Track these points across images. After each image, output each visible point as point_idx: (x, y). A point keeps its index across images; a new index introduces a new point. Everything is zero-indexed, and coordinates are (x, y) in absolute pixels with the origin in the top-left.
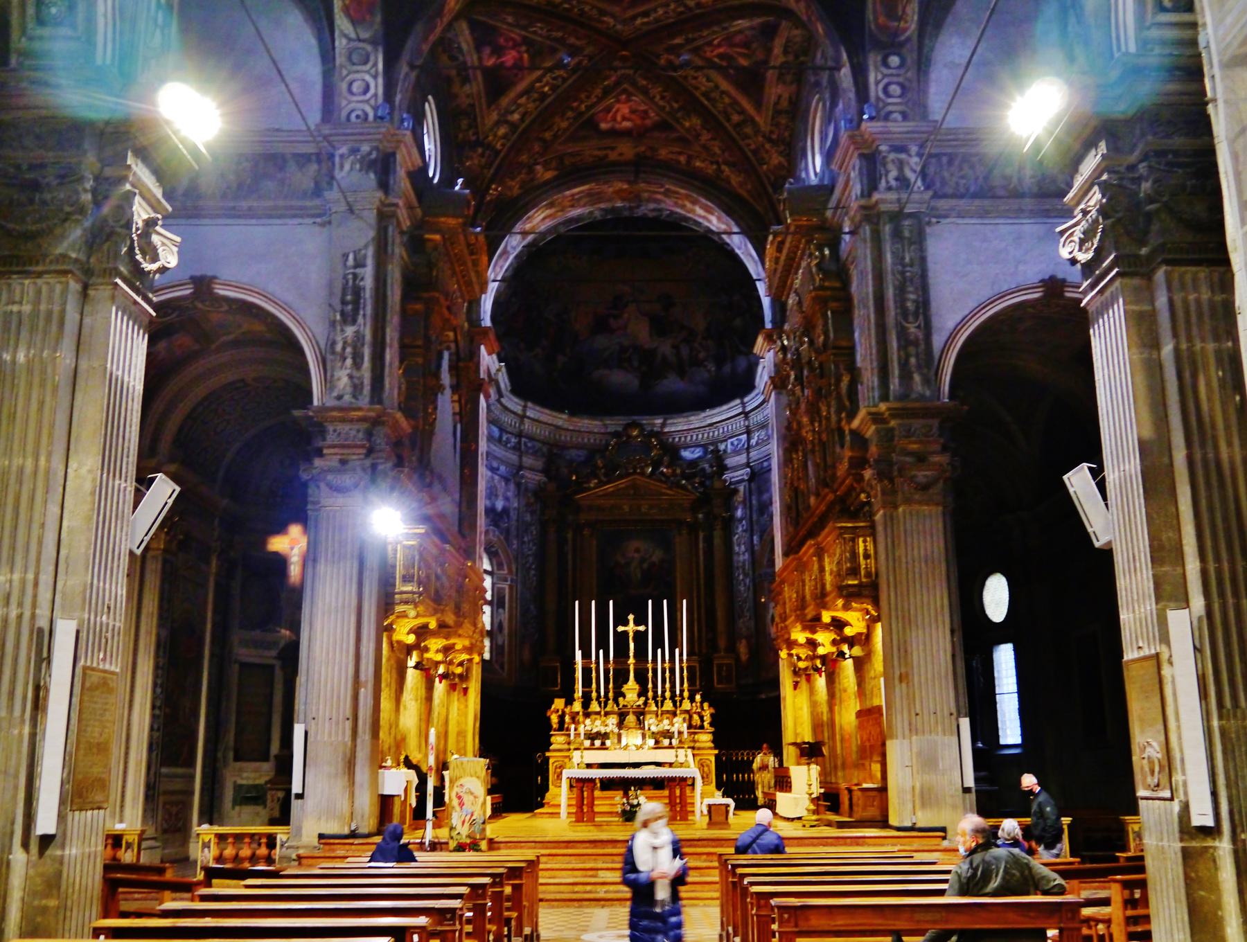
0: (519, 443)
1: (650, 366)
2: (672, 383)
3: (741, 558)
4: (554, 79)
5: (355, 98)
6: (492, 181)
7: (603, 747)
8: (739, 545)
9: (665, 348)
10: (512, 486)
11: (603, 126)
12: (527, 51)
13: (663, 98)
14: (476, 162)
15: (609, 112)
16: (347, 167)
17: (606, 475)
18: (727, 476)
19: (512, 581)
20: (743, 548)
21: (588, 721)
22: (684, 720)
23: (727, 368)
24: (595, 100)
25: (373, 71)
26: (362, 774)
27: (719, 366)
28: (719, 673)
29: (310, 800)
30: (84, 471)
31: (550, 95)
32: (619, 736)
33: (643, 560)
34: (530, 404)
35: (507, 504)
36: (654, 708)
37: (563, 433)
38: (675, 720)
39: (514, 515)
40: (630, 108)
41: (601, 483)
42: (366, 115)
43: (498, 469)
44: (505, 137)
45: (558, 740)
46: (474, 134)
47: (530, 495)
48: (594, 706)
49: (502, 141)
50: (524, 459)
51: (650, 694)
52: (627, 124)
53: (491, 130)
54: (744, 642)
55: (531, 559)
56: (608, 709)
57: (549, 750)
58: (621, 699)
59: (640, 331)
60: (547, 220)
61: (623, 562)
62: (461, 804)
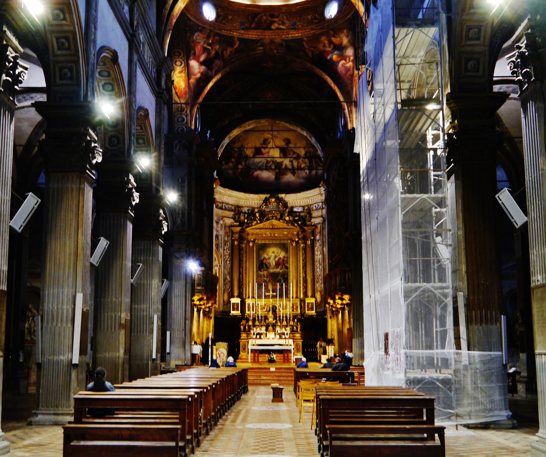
1: (280, 170)
2: (289, 177)
3: (318, 257)
5: (179, 123)
7: (260, 338)
8: (318, 251)
9: (286, 162)
16: (178, 148)
17: (259, 220)
18: (313, 220)
19: (219, 266)
20: (319, 252)
21: (254, 329)
22: (290, 329)
23: (314, 172)
25: (186, 114)
26: (187, 347)
27: (310, 172)
28: (308, 306)
29: (172, 356)
30: (156, 283)
32: (266, 334)
33: (275, 257)
36: (279, 324)
37: (241, 200)
38: (287, 328)
41: (257, 223)
42: (183, 129)
45: (244, 335)
48: (257, 323)
51: (278, 318)
54: (319, 293)
55: (227, 257)
56: (262, 324)
57: (240, 339)
58: (267, 321)
59: (276, 153)
61: (267, 257)
62: (220, 356)
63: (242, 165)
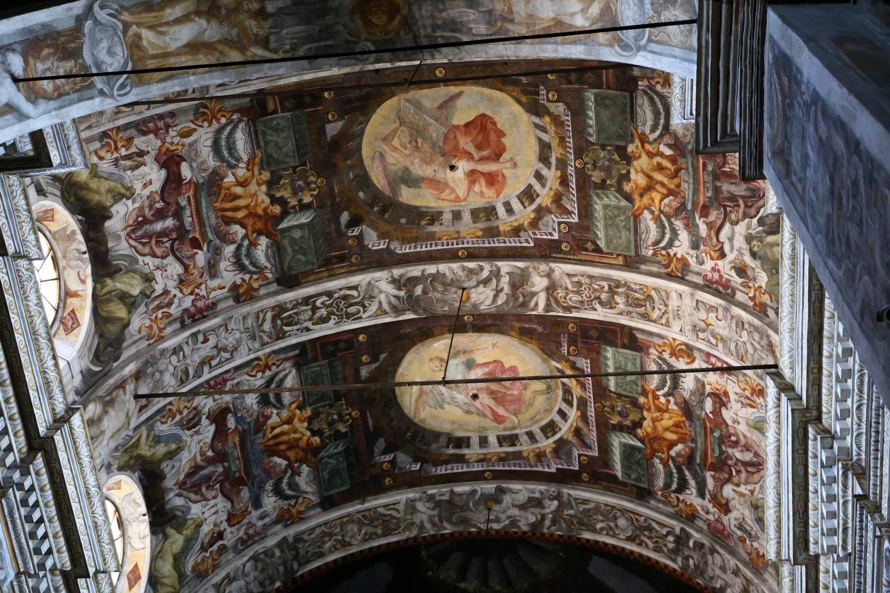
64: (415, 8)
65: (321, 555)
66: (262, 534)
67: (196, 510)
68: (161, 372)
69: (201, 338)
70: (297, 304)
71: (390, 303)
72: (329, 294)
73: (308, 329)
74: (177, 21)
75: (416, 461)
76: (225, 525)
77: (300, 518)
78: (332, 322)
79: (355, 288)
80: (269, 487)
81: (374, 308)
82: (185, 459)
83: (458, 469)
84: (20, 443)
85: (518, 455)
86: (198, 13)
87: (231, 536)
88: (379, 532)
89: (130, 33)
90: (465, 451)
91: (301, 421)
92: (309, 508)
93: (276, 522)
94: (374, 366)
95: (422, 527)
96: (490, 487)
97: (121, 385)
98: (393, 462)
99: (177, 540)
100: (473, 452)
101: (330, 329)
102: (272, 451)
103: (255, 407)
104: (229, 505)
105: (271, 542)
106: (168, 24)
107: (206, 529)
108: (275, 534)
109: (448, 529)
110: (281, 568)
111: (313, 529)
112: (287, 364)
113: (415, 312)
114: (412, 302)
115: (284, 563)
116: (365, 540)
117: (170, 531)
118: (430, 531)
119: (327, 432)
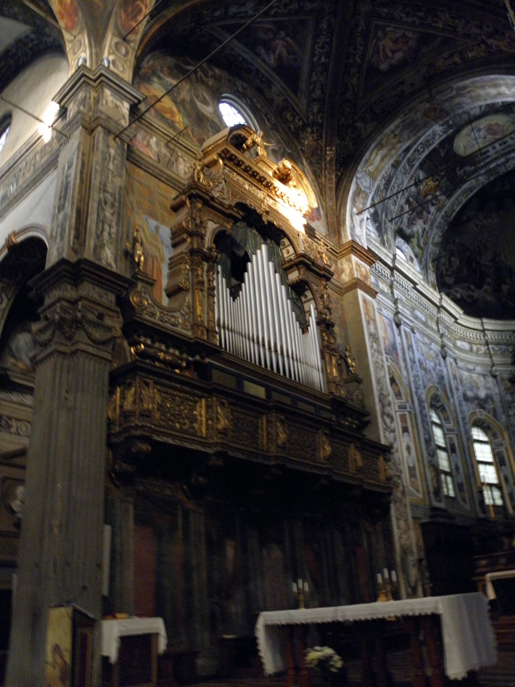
0: (488, 349)
4: (322, 48)
6: (326, 147)
10: (490, 379)
11: (384, 67)
12: (287, 35)
13: (407, 14)
14: (311, 138)
15: (378, 53)
24: (362, 48)
31: (329, 63)
34: (485, 320)
35: (489, 392)
39: (497, 399)
40: (391, 39)
43: (474, 369)
44: (319, 111)
46: (299, 121)
47: (506, 382)
49: (319, 115)
50: (494, 358)
52: (399, 55)
53: (308, 111)
60: (386, 160)
63: (507, 284)
64: (443, 106)
65: (454, 211)
66: (435, 220)
67: (415, 229)
68: (390, 208)
69: (393, 188)
70: (413, 154)
71: (443, 132)
72: (421, 144)
73: (419, 158)
74: (375, 157)
75: (471, 166)
76: (424, 226)
77: (443, 206)
78: (426, 150)
79: (429, 136)
80: (430, 205)
81: (438, 136)
82: (405, 220)
83: (488, 160)
84: (388, 272)
85: (510, 146)
86: (379, 150)
87: (427, 227)
88: (469, 192)
89: (367, 172)
90: (488, 154)
91: (429, 182)
92: (444, 202)
93: (437, 212)
94: (444, 151)
95: (483, 183)
96: (503, 160)
97: (385, 223)
98: (465, 172)
99: (415, 241)
100: (492, 152)
101: (427, 152)
102: (426, 195)
103: (415, 189)
104: (422, 220)
105: (439, 219)
106: (373, 160)
107: (420, 231)
108: (439, 216)
109: (492, 178)
110: (445, 223)
111: (448, 207)
112: (418, 171)
113: (452, 128)
114: (449, 127)
115: (445, 221)
116: (465, 198)
117: (412, 240)
118: (486, 182)
119: (439, 178)
